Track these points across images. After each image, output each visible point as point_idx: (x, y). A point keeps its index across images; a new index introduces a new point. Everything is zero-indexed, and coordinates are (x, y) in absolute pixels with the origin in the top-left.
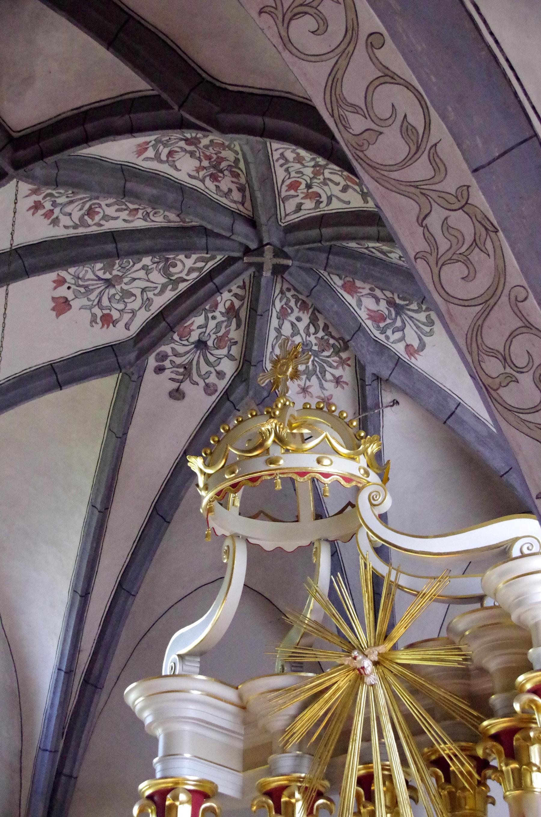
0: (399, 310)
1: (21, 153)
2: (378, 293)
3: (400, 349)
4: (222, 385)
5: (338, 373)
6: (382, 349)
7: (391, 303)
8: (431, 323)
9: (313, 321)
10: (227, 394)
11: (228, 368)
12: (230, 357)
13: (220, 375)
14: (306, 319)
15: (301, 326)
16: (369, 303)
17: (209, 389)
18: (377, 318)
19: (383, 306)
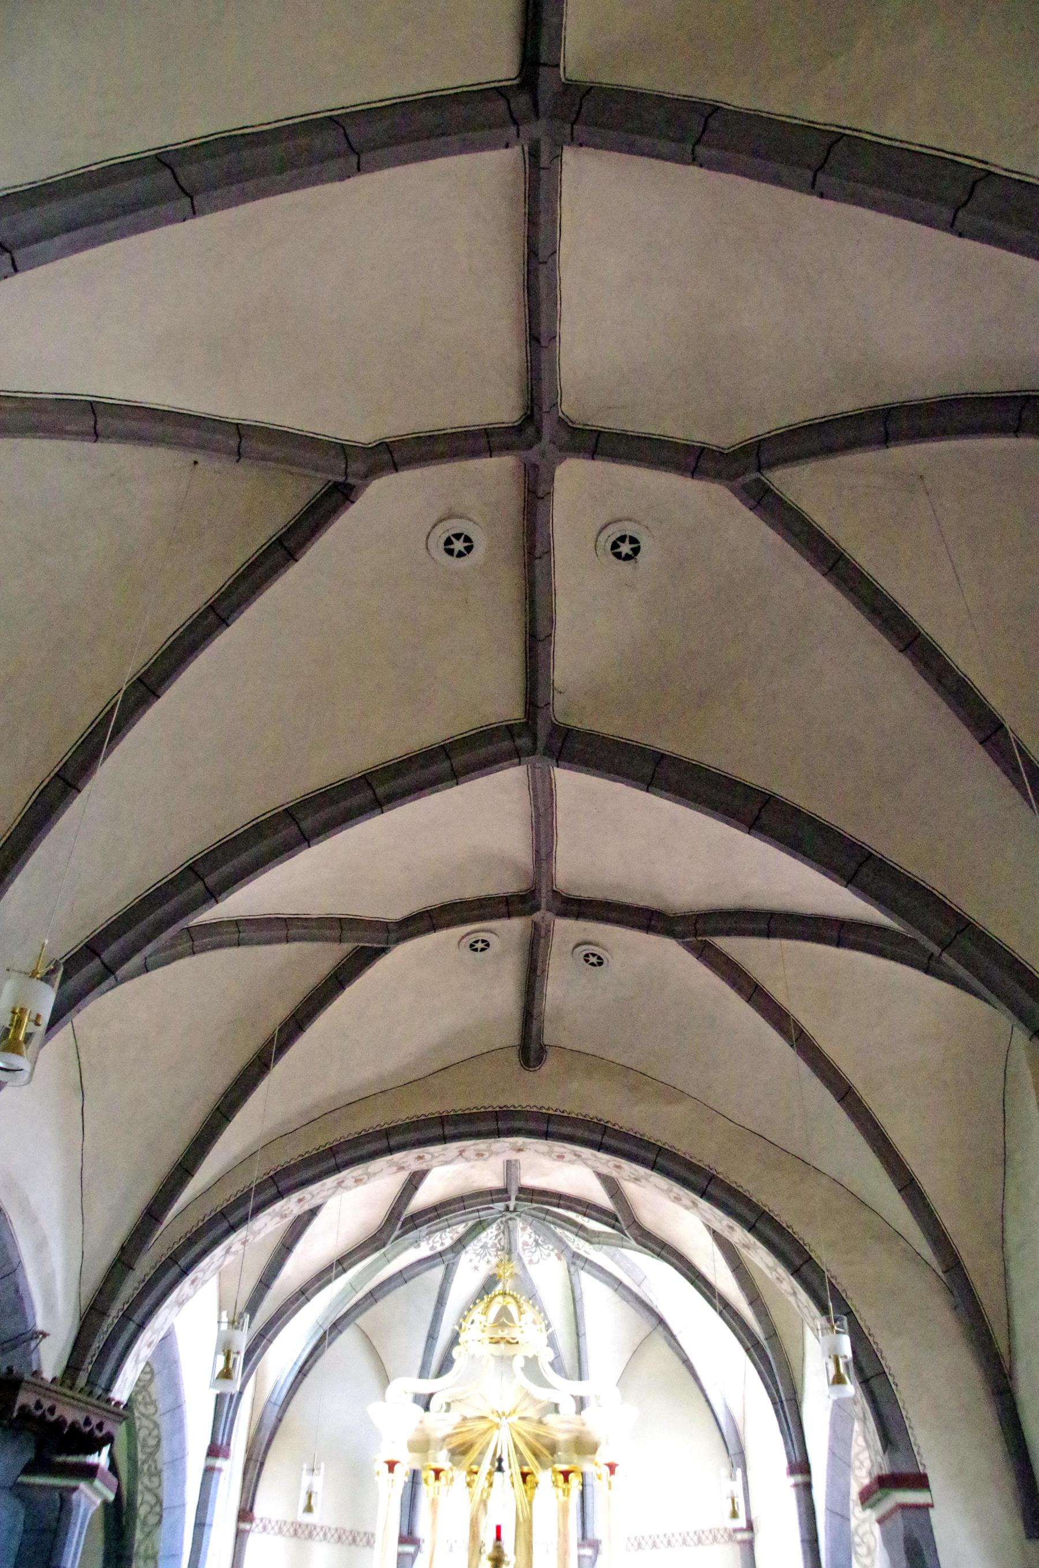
0: (537, 1244)
1: (521, 1195)
2: (533, 1235)
3: (526, 1260)
4: (439, 1248)
5: (490, 1258)
6: (520, 1258)
7: (536, 1241)
8: (549, 1255)
9: (497, 1236)
10: (441, 1254)
11: (448, 1242)
12: (452, 1238)
13: (442, 1244)
14: (495, 1233)
15: (490, 1235)
16: (526, 1237)
17: (432, 1248)
18: (525, 1244)
19: (531, 1241)
